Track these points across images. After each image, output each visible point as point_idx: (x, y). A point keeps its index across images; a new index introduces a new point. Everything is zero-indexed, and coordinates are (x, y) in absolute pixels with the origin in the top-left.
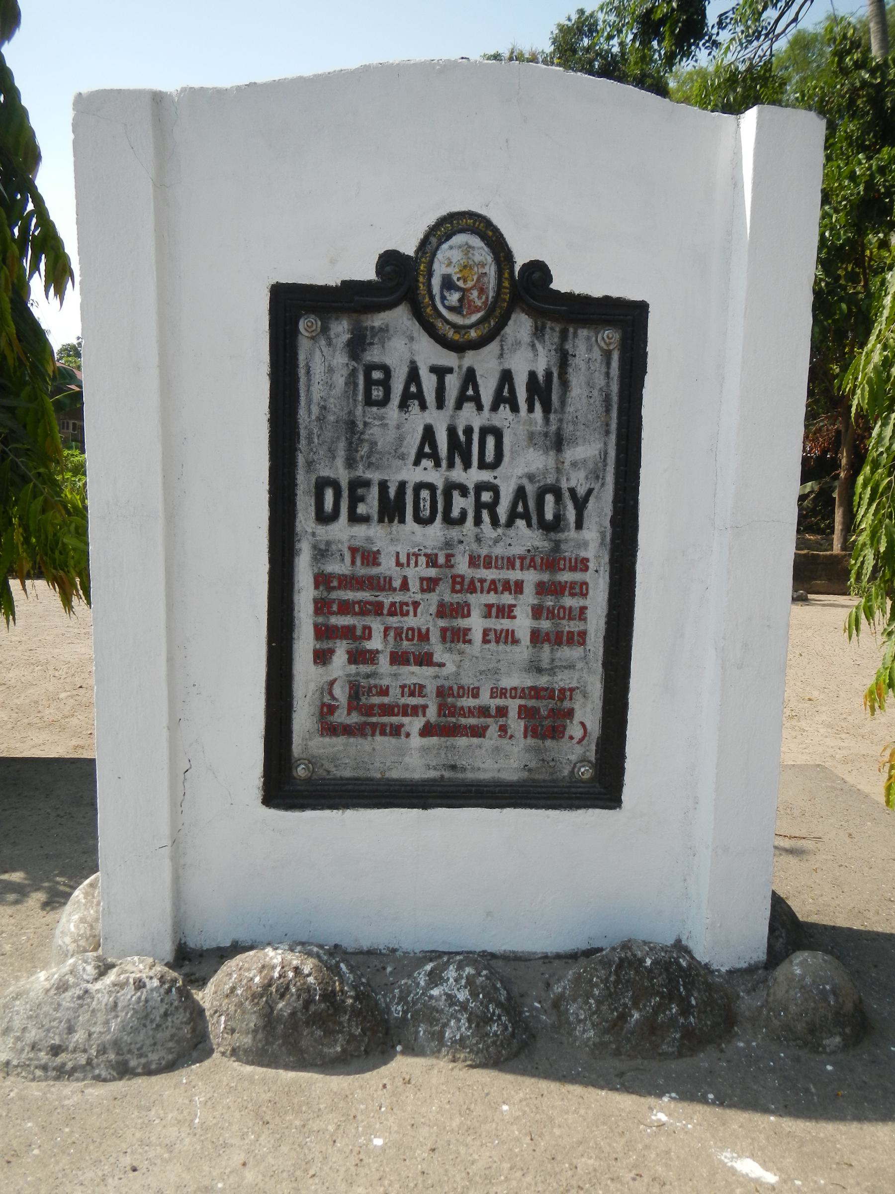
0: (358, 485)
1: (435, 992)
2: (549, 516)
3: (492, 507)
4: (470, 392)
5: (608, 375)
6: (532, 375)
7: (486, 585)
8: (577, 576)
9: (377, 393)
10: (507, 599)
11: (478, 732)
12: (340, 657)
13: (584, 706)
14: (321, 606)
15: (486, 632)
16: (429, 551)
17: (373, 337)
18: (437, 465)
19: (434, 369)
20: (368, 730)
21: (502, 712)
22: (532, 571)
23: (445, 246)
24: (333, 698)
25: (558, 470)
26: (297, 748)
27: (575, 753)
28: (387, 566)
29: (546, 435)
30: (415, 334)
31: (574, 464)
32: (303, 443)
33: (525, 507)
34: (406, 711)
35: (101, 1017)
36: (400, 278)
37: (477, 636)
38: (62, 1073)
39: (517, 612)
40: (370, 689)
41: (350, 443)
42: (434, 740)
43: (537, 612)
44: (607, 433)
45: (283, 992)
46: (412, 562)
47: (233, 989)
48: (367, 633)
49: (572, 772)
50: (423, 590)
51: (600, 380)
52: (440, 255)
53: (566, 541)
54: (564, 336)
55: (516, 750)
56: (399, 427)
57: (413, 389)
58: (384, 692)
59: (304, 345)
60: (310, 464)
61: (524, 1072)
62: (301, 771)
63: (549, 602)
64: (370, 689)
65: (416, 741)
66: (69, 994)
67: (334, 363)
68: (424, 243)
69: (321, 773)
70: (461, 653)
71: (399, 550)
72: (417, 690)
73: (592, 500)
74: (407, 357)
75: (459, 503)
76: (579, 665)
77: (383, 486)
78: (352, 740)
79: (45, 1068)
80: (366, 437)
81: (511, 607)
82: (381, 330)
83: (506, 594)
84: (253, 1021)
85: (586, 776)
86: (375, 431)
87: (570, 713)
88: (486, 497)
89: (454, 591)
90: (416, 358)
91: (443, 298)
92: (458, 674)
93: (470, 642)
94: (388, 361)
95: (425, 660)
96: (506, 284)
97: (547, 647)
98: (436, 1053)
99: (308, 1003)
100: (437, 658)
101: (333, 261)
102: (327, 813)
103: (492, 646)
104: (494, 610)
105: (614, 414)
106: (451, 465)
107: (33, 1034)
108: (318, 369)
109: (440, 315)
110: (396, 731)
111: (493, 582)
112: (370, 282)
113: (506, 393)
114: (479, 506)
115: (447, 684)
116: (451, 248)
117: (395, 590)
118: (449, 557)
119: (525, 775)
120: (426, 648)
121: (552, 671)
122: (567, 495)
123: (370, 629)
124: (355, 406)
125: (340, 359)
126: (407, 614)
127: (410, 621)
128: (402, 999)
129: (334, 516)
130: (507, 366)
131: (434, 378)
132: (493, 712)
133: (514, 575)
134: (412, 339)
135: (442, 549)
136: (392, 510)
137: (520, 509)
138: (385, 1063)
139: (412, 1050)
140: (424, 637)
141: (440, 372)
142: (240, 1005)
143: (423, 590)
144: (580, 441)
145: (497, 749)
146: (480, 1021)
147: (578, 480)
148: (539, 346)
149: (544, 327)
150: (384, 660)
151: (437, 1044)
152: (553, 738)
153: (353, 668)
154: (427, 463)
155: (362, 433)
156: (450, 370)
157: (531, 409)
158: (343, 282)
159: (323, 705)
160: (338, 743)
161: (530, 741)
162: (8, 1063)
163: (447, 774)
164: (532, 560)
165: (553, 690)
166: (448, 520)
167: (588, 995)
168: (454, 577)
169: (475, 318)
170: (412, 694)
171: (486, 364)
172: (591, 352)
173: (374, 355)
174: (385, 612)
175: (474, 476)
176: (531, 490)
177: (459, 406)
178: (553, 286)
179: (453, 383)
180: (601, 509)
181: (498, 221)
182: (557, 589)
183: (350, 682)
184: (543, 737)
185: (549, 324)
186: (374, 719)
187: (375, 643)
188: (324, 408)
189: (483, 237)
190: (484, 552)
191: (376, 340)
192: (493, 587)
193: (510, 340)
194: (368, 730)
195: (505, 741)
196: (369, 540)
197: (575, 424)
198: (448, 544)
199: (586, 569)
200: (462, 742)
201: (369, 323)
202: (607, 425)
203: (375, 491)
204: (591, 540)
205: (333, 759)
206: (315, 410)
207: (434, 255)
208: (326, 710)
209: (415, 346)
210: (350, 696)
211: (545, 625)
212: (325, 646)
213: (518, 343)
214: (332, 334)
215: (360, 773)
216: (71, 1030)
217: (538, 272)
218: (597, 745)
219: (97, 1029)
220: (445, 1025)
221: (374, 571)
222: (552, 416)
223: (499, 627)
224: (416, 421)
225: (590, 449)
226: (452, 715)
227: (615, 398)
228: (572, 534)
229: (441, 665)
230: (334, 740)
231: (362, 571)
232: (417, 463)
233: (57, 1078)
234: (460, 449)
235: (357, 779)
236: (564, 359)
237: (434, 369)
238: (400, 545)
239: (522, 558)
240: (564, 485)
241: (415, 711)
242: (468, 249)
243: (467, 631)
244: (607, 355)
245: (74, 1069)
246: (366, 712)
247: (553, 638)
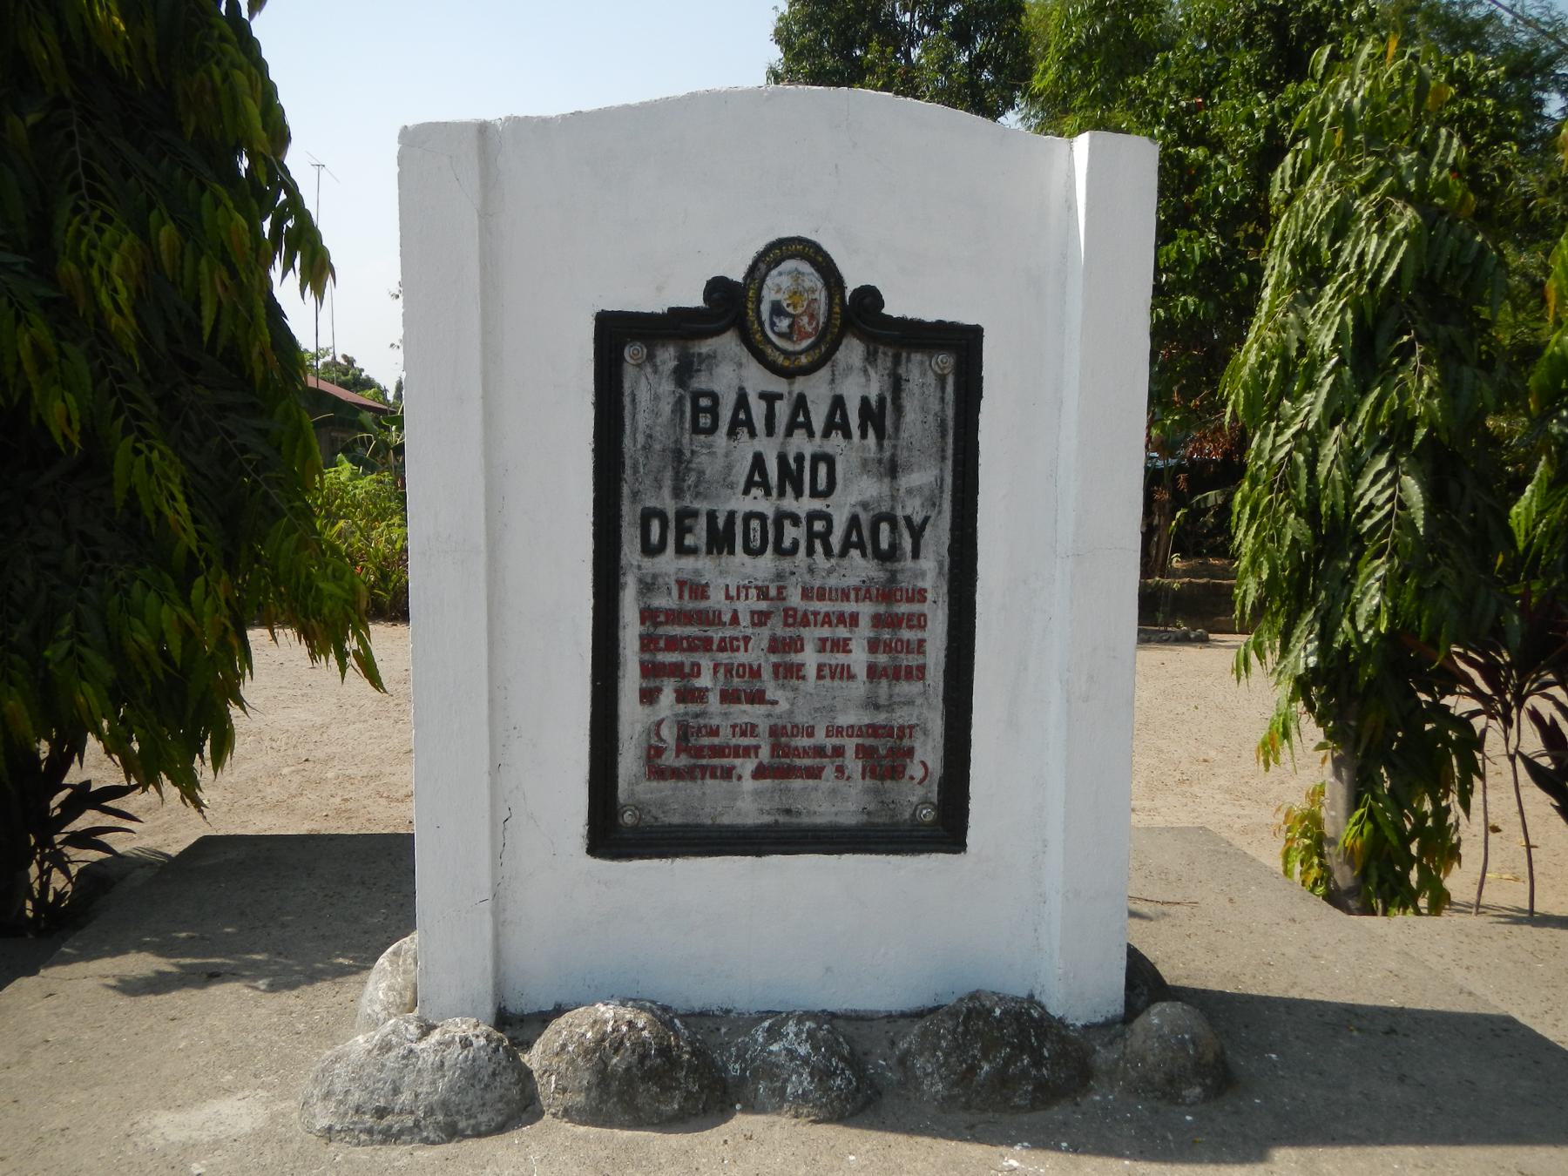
0: (685, 515)
1: (775, 1047)
2: (884, 545)
3: (825, 537)
4: (801, 419)
5: (942, 399)
6: (865, 401)
7: (820, 618)
8: (915, 608)
9: (705, 421)
10: (842, 632)
11: (814, 773)
12: (667, 697)
13: (924, 744)
14: (648, 643)
15: (820, 668)
16: (760, 583)
17: (700, 363)
18: (768, 493)
19: (762, 396)
20: (698, 773)
21: (839, 751)
22: (868, 602)
23: (774, 272)
24: (662, 740)
25: (893, 498)
26: (622, 795)
27: (915, 794)
28: (716, 599)
29: (880, 461)
30: (744, 361)
31: (909, 492)
32: (628, 473)
33: (859, 536)
34: (739, 752)
35: (427, 1077)
36: (728, 304)
37: (811, 671)
38: (389, 1137)
39: (853, 645)
40: (699, 729)
41: (677, 473)
42: (767, 783)
43: (873, 646)
44: (943, 458)
45: (618, 1047)
46: (743, 595)
47: (563, 1047)
48: (696, 670)
49: (914, 814)
50: (754, 625)
51: (935, 406)
52: (769, 282)
53: (903, 571)
54: (897, 361)
55: (853, 792)
57: (742, 416)
58: (714, 732)
59: (629, 372)
60: (635, 495)
61: (871, 1127)
62: (628, 818)
63: (886, 635)
64: (699, 729)
65: (748, 784)
66: (393, 1054)
67: (661, 390)
68: (753, 269)
69: (648, 819)
70: (795, 689)
71: (728, 581)
72: (749, 730)
73: (928, 528)
74: (735, 383)
75: (790, 533)
76: (919, 701)
77: (712, 516)
78: (681, 784)
79: (370, 1131)
80: (693, 466)
81: (846, 641)
82: (709, 356)
83: (841, 627)
84: (586, 1078)
85: (928, 819)
86: (702, 460)
87: (910, 752)
88: (819, 526)
89: (786, 624)
90: (745, 385)
91: (773, 324)
92: (791, 712)
93: (803, 678)
94: (716, 388)
95: (757, 697)
96: (837, 309)
97: (884, 682)
98: (777, 1110)
99: (644, 1057)
100: (769, 695)
101: (659, 289)
102: (656, 862)
103: (827, 682)
104: (828, 645)
105: (950, 440)
106: (782, 494)
107: (356, 1097)
108: (644, 396)
109: (770, 342)
110: (727, 773)
111: (827, 615)
112: (697, 309)
113: (838, 419)
114: (811, 535)
115: (780, 722)
116: (780, 274)
117: (724, 624)
118: (780, 589)
119: (864, 818)
120: (758, 685)
121: (890, 708)
122: (902, 523)
123: (699, 666)
124: (682, 434)
125: (667, 387)
126: (738, 649)
127: (741, 657)
128: (740, 1057)
129: (661, 548)
130: (838, 392)
131: (763, 404)
132: (829, 752)
133: (849, 607)
134: (740, 365)
135: (773, 581)
136: (720, 541)
137: (854, 538)
138: (726, 1122)
139: (752, 1108)
140: (756, 673)
141: (770, 398)
142: (572, 1062)
143: (754, 625)
144: (915, 467)
145: (834, 792)
146: (823, 1075)
147: (913, 508)
148: (872, 372)
149: (876, 352)
150: (714, 699)
151: (777, 1101)
152: (893, 778)
153: (681, 708)
154: (756, 492)
155: (690, 462)
156: (780, 397)
157: (864, 435)
158: (671, 310)
159: (650, 747)
160: (666, 787)
161: (869, 782)
162: (330, 1128)
163: (782, 819)
164: (868, 591)
165: (892, 728)
166: (780, 551)
167: (936, 1047)
168: (786, 610)
169: (805, 344)
170: (743, 734)
171: (818, 390)
172: (924, 379)
173: (701, 382)
174: (715, 647)
175: (806, 504)
176: (865, 518)
177: (789, 433)
178: (886, 311)
179: (783, 409)
180: (938, 537)
181: (827, 246)
182: (894, 622)
183: (678, 722)
184: (882, 778)
185: (881, 349)
186: (704, 762)
187: (705, 681)
188: (650, 436)
189: (813, 263)
190: (817, 583)
191: (704, 367)
192: (827, 620)
193: (841, 366)
194: (698, 773)
195: (842, 783)
196: (697, 572)
197: (910, 450)
198: (780, 576)
199: (924, 600)
200: (797, 784)
201: (696, 350)
202: (943, 450)
203: (703, 522)
204: (928, 569)
205: (662, 804)
206: (641, 439)
207: (763, 281)
208: (653, 753)
209: (744, 373)
210: (678, 738)
211: (882, 659)
212: (652, 684)
213: (850, 368)
214: (658, 361)
215: (691, 820)
216: (396, 1091)
217: (869, 297)
218: (940, 785)
219: (425, 1089)
220: (786, 1081)
221: (703, 605)
222: (886, 442)
223: (833, 662)
224: (746, 448)
225: (925, 476)
226: (786, 755)
227: (951, 424)
228: (908, 563)
229: (774, 703)
230: (662, 784)
231: (689, 605)
232: (746, 492)
233: (383, 1142)
234: (791, 477)
235: (687, 826)
236: (897, 384)
237: (762, 396)
238: (732, 576)
239: (857, 590)
240: (899, 513)
241: (747, 752)
242: (797, 275)
243: (801, 666)
244: (942, 379)
245: (401, 1132)
246: (697, 754)
247: (890, 672)
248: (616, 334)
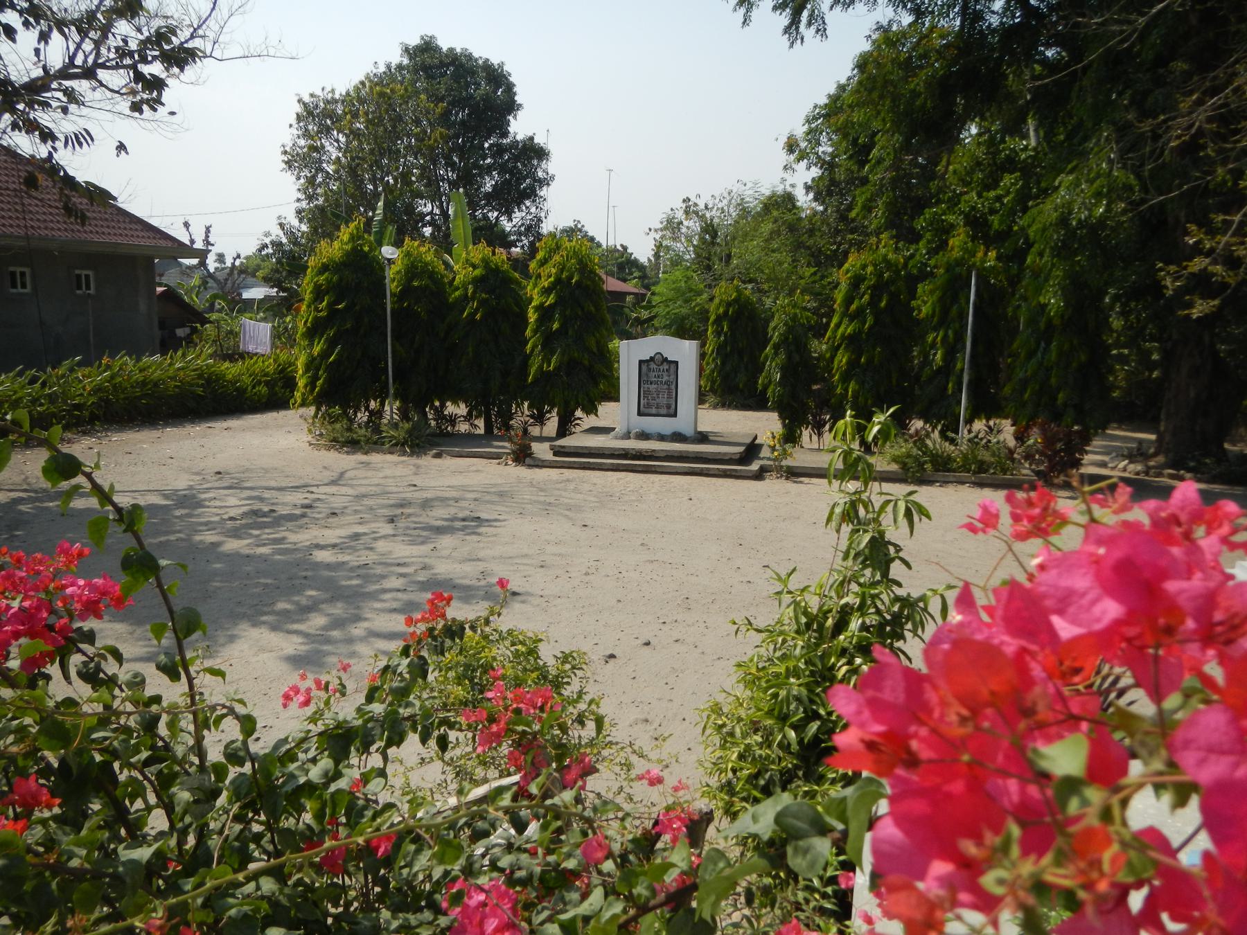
27: (672, 411)
36: (652, 359)
172: (673, 366)
204: (673, 387)
225: (673, 377)
246: (648, 406)
248: (641, 362)
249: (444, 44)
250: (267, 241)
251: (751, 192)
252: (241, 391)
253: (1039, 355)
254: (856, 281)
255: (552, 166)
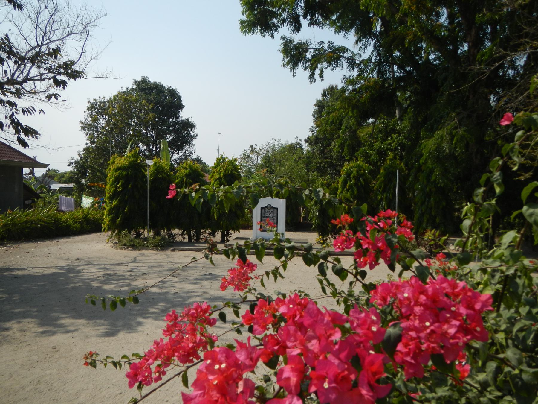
33: (272, 217)
36: (266, 207)
56: (266, 213)
172: (275, 210)
225: (275, 214)
248: (262, 208)
249: (152, 80)
250: (73, 161)
251: (277, 143)
252: (69, 226)
253: (426, 203)
254: (348, 175)
255: (196, 131)
